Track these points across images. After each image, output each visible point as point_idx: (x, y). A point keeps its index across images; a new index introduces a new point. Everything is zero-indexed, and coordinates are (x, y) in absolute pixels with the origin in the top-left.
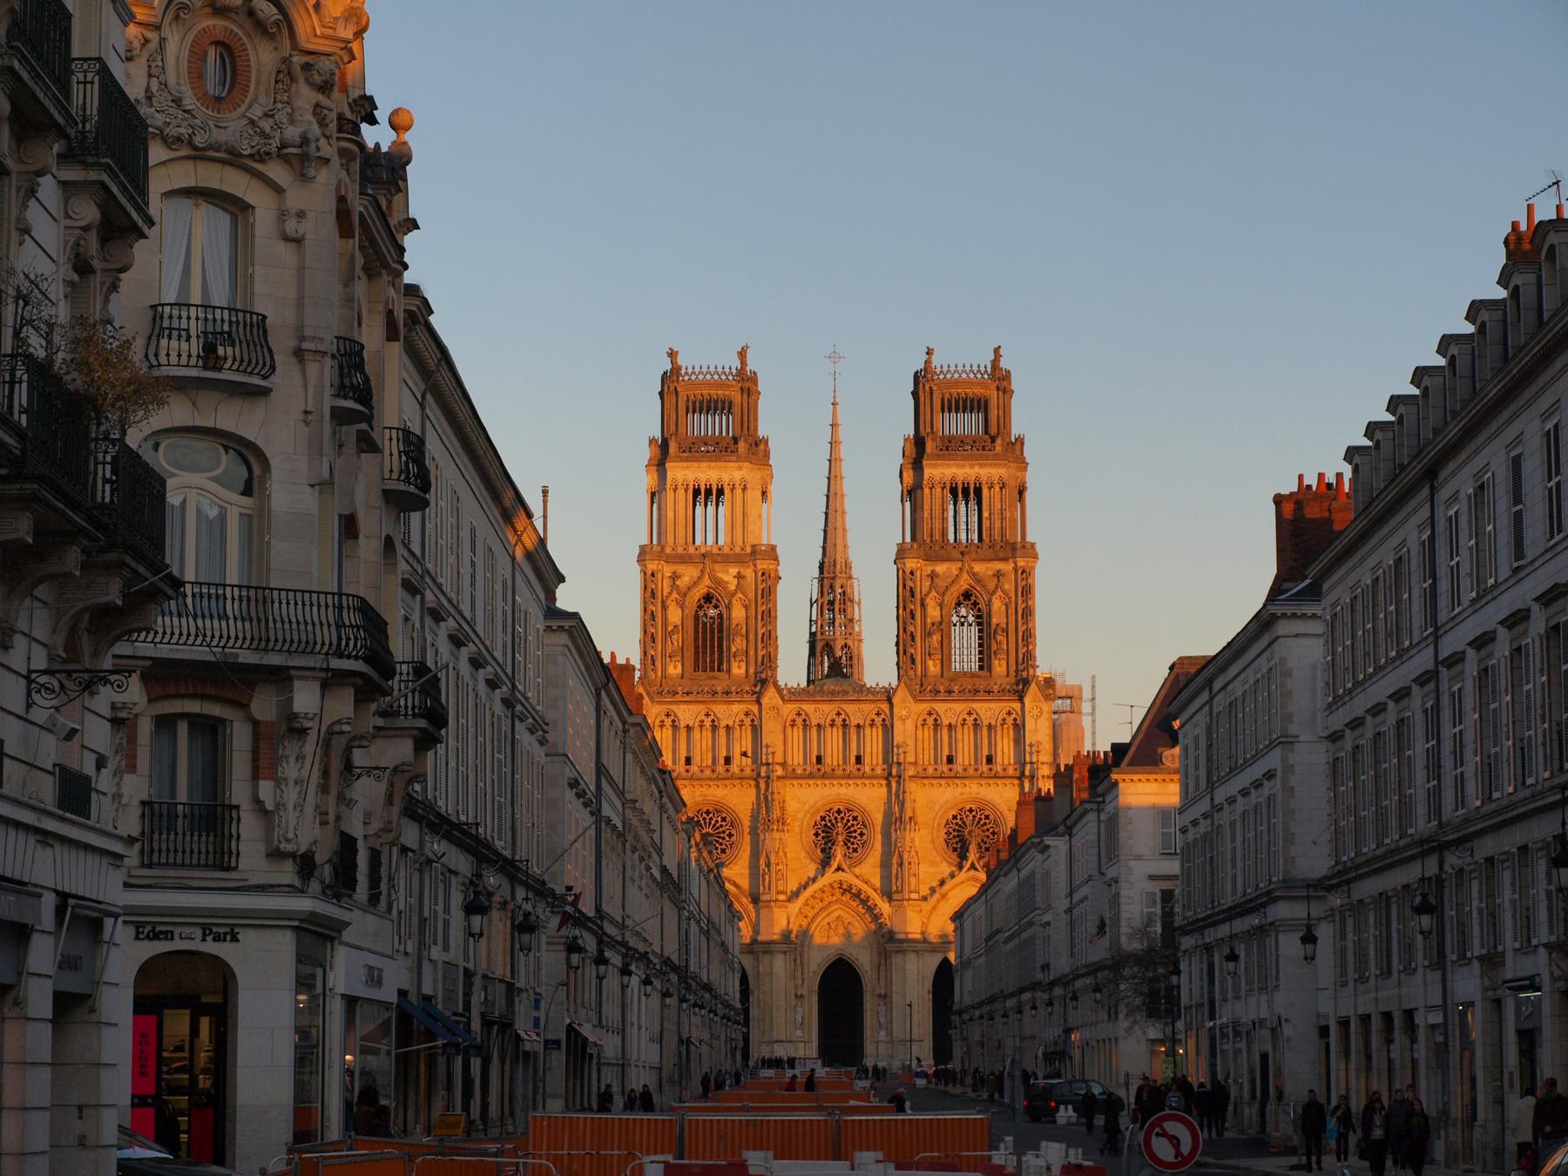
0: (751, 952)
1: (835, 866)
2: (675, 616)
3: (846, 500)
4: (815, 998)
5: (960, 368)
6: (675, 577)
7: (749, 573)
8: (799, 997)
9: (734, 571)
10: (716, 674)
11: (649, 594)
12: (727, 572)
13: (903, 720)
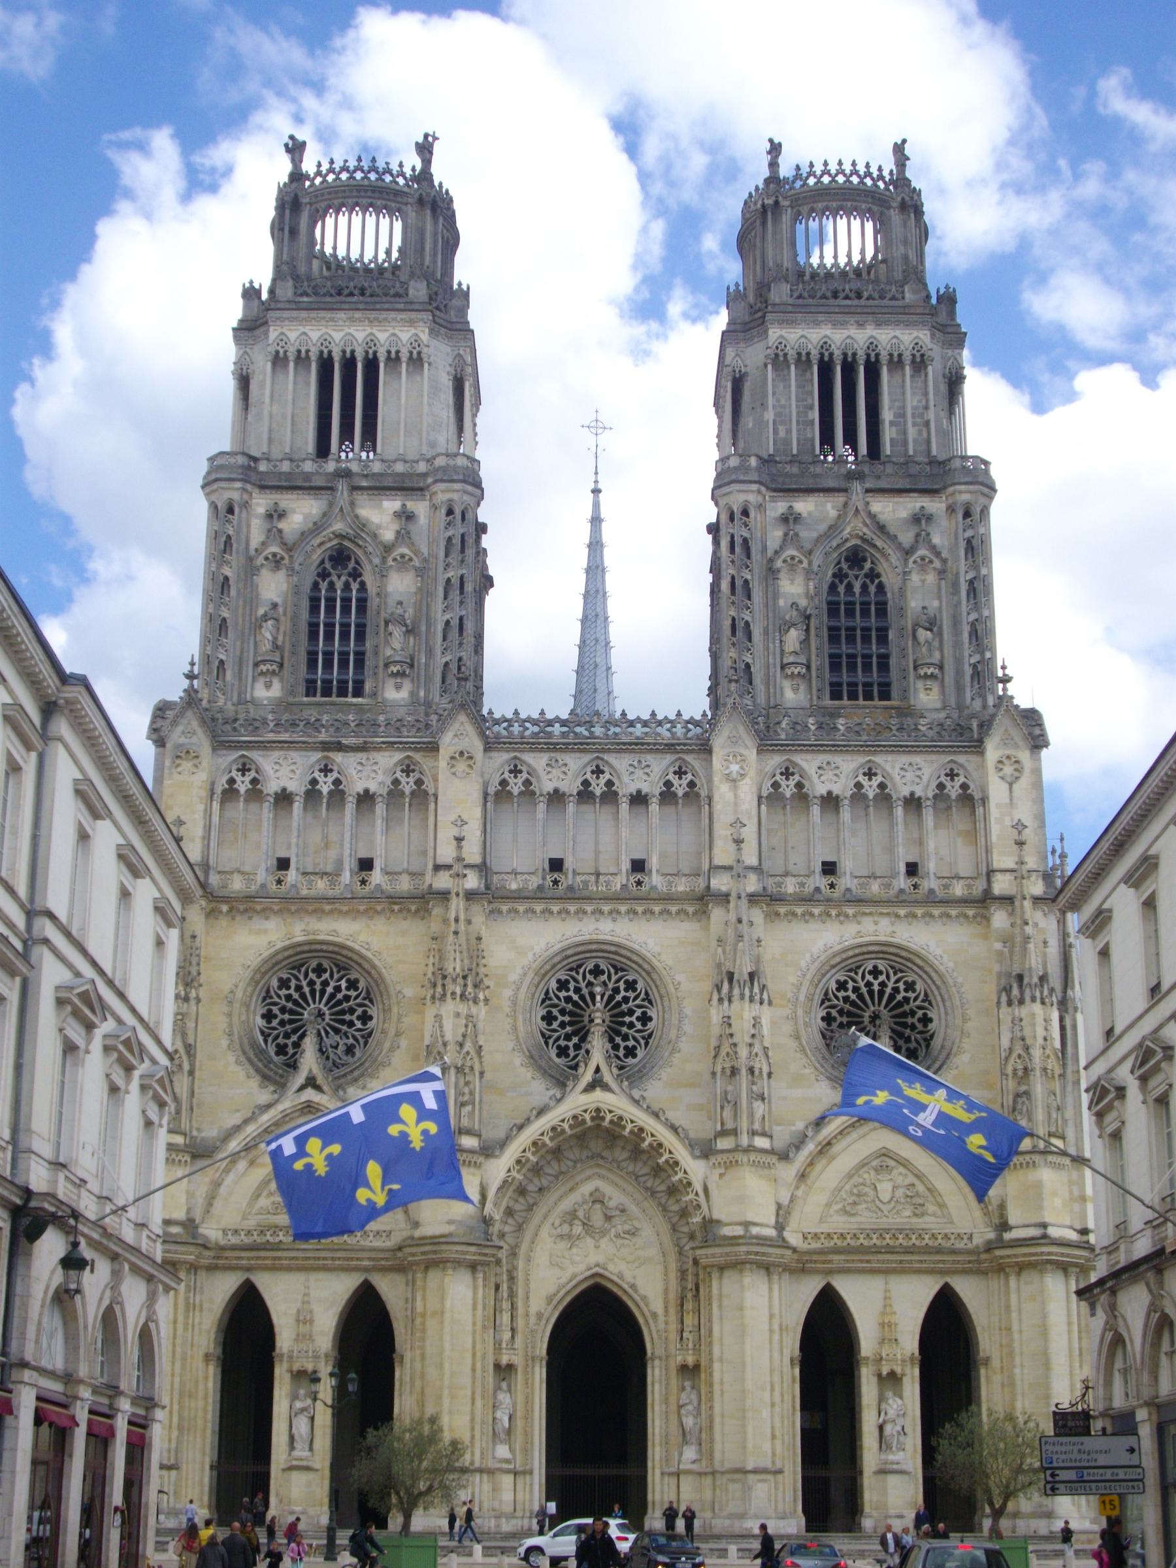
0: (400, 1269)
1: (588, 1077)
2: (273, 587)
3: (606, 551)
4: (539, 1374)
5: (833, 168)
6: (275, 515)
7: (420, 508)
8: (504, 1371)
9: (392, 505)
10: (351, 700)
11: (223, 544)
12: (380, 507)
13: (733, 781)
